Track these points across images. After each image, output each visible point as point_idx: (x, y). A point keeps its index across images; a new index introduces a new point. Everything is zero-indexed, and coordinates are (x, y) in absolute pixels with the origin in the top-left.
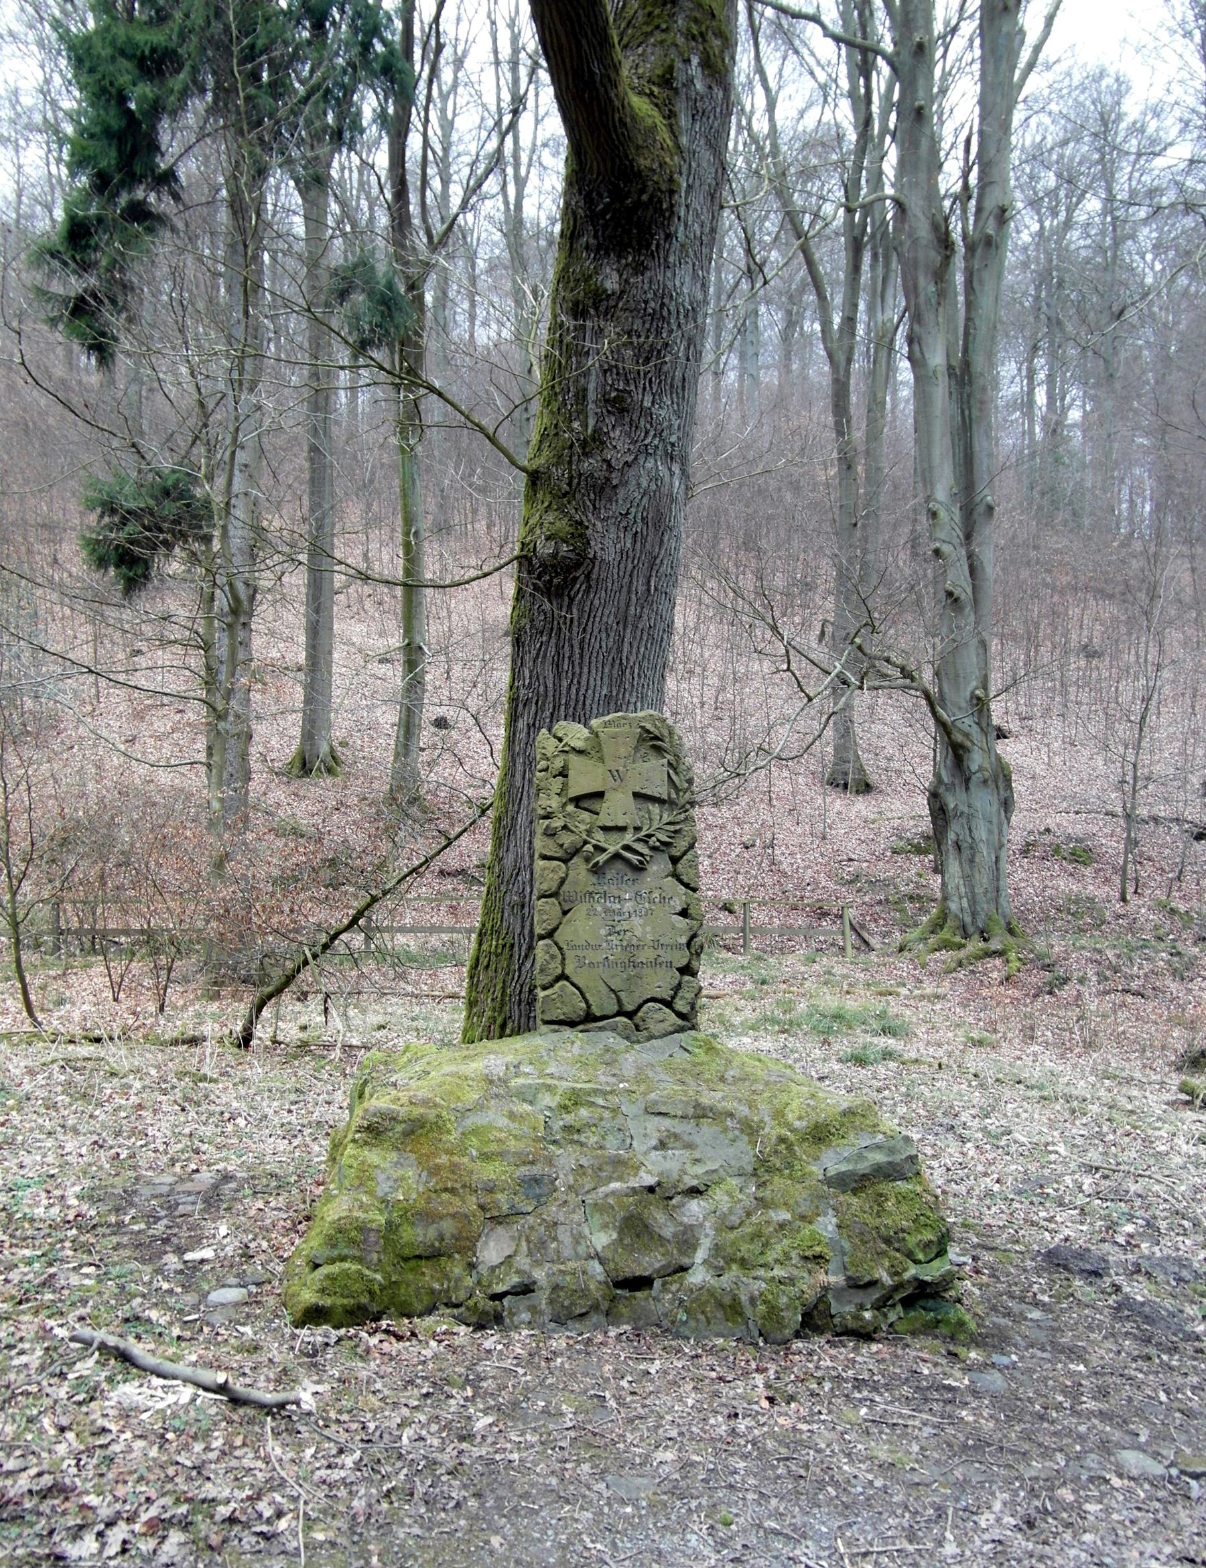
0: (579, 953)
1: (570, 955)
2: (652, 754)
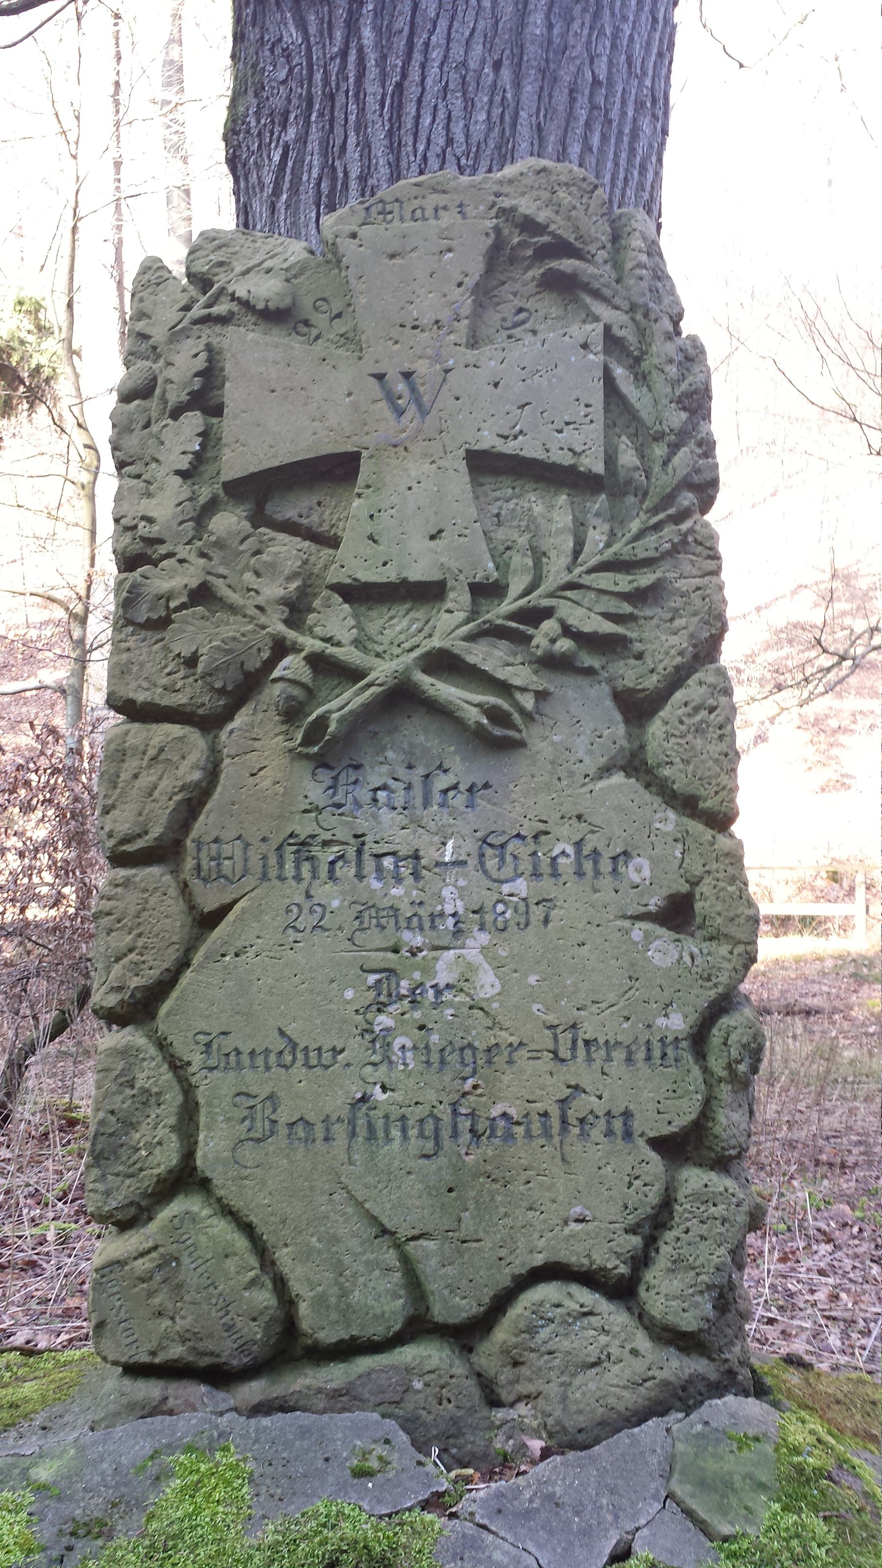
0: (258, 1083)
1: (214, 1088)
2: (547, 305)
